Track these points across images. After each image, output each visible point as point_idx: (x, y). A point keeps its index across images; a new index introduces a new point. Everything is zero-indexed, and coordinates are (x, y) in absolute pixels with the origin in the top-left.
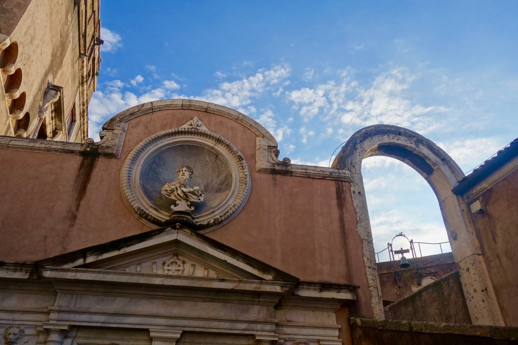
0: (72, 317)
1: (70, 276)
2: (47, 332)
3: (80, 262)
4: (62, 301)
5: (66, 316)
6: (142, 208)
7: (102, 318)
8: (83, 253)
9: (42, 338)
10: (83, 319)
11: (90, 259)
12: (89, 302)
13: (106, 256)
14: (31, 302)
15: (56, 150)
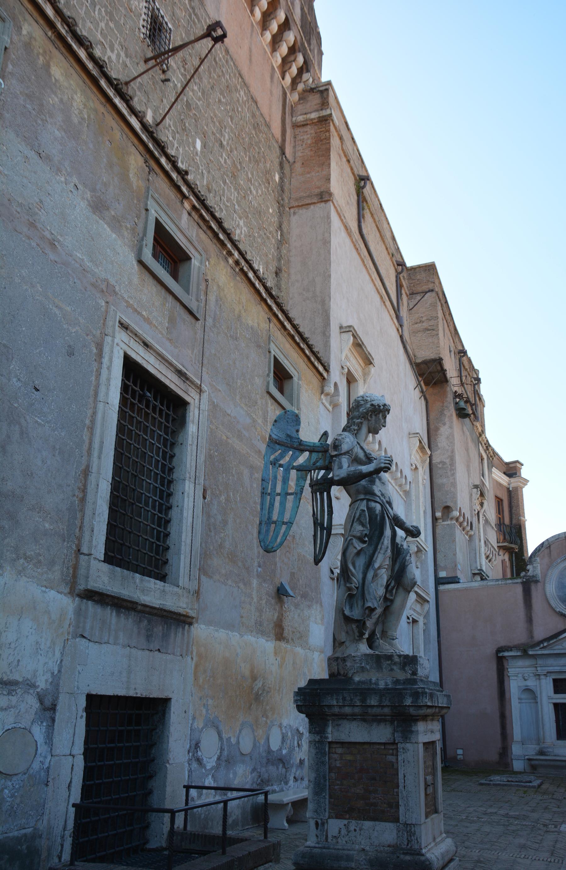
0: (546, 668)
1: (540, 652)
2: (539, 675)
3: (542, 646)
4: (540, 662)
5: (544, 668)
6: (561, 611)
7: (559, 668)
8: (542, 642)
9: (537, 677)
10: (551, 669)
11: (545, 644)
12: (550, 661)
13: (551, 642)
14: (527, 662)
15: (510, 584)
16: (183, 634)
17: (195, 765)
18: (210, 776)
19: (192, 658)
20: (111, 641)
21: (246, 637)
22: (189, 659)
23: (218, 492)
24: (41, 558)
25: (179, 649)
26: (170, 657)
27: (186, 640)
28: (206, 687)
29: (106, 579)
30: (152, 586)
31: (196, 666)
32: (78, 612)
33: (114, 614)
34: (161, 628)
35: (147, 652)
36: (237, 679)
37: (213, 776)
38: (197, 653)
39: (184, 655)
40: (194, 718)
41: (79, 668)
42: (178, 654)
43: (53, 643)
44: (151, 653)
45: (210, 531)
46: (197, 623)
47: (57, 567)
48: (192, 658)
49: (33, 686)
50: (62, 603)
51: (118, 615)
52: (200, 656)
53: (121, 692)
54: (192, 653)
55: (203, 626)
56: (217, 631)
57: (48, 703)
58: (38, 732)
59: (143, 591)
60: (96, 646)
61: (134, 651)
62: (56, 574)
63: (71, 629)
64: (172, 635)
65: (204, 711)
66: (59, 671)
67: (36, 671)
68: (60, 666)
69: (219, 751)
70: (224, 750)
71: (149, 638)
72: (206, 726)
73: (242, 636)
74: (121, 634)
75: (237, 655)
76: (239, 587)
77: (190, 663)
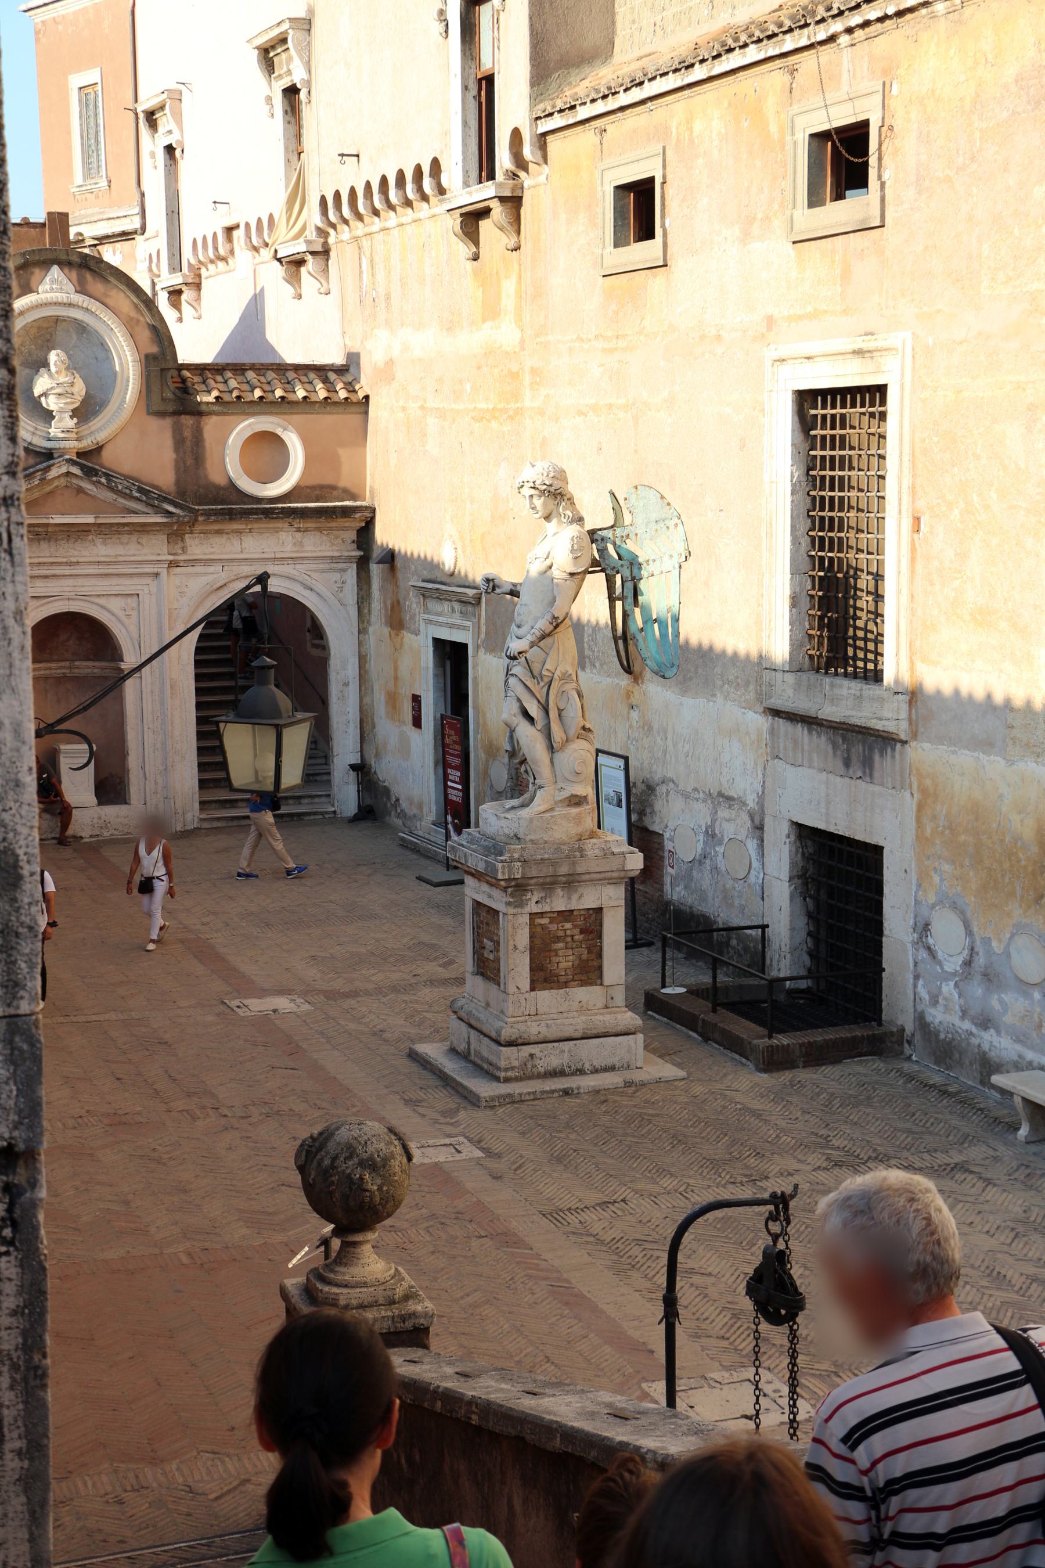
16: (893, 757)
17: (923, 954)
18: (952, 984)
19: (912, 794)
20: (806, 763)
21: (1021, 766)
22: (907, 794)
23: (944, 509)
24: (739, 680)
25: (890, 779)
26: (877, 789)
27: (897, 768)
28: (938, 842)
29: (790, 692)
30: (844, 692)
31: (920, 807)
32: (772, 731)
33: (806, 732)
34: (861, 747)
35: (847, 780)
36: (1002, 841)
37: (956, 985)
38: (918, 787)
39: (898, 787)
40: (919, 886)
41: (779, 791)
42: (890, 785)
43: (756, 764)
44: (853, 782)
45: (932, 584)
46: (916, 740)
47: (751, 687)
48: (912, 794)
49: (744, 804)
50: (758, 722)
51: (810, 731)
52: (924, 791)
53: (822, 826)
54: (911, 787)
55: (926, 745)
56: (954, 752)
57: (757, 822)
58: (752, 845)
59: (834, 701)
60: (792, 769)
61: (831, 777)
62: (751, 695)
63: (769, 750)
64: (877, 757)
65: (936, 879)
66: (763, 792)
67: (745, 790)
68: (763, 787)
69: (966, 952)
70: (977, 953)
71: (847, 763)
72: (940, 902)
73: (1011, 763)
74: (815, 757)
75: (1001, 796)
76: (1001, 671)
77: (909, 802)
